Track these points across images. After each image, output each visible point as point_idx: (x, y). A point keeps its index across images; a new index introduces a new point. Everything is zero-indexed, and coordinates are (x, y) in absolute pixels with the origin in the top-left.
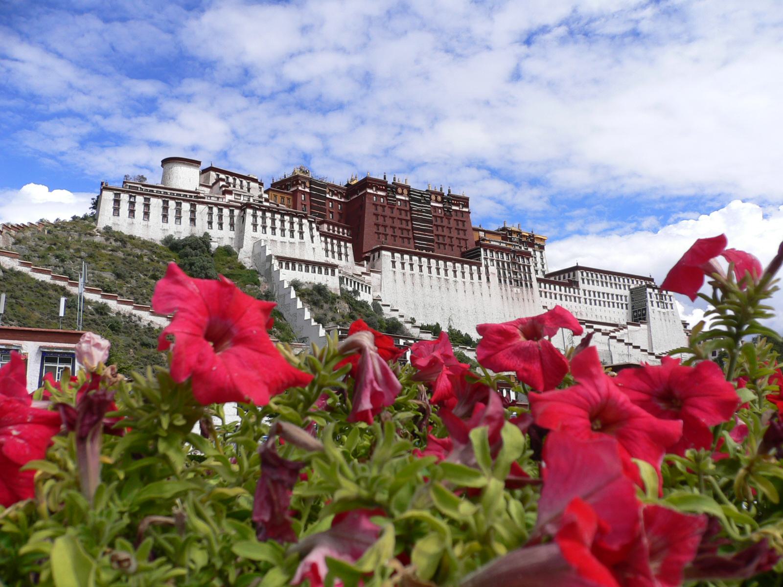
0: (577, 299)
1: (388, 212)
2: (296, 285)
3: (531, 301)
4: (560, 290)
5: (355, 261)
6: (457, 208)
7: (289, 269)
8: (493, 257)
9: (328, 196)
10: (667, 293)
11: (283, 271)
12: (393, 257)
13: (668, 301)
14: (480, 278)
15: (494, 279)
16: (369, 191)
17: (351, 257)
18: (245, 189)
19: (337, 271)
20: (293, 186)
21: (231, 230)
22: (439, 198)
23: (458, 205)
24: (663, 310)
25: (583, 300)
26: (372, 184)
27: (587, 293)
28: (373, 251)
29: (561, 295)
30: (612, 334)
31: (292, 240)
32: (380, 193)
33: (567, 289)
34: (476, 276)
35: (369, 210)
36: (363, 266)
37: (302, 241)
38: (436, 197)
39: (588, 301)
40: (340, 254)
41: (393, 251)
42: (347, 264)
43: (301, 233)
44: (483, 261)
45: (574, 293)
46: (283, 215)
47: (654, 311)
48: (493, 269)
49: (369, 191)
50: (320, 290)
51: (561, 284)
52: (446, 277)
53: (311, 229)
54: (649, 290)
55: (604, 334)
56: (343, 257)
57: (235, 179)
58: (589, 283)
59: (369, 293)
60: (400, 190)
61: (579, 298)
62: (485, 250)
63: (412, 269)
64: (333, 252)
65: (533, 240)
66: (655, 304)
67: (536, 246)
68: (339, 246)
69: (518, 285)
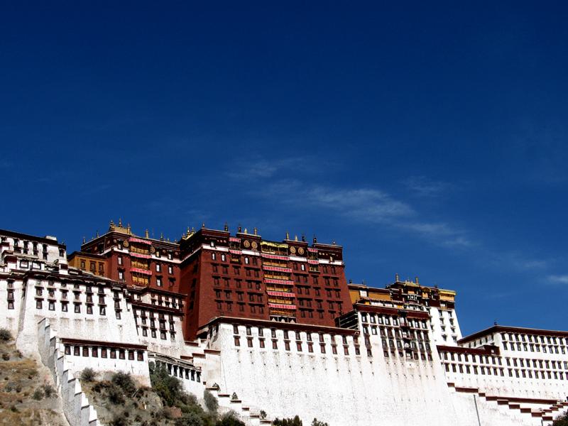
0: (498, 371)
2: (88, 376)
3: (431, 377)
4: (474, 361)
5: (185, 339)
6: (326, 262)
7: (124, 358)
8: (375, 322)
9: (154, 257)
11: (71, 358)
12: (236, 331)
15: (377, 350)
16: (206, 247)
17: (179, 335)
18: (40, 255)
19: (145, 355)
20: (108, 246)
21: (9, 308)
25: (506, 372)
26: (208, 237)
27: (512, 361)
28: (210, 325)
29: (475, 367)
30: (548, 414)
31: (89, 317)
32: (219, 249)
33: (484, 358)
34: (352, 349)
35: (206, 271)
36: (196, 345)
37: (104, 317)
38: (297, 249)
39: (514, 372)
40: (163, 331)
41: (236, 323)
42: (175, 346)
43: (102, 306)
44: (361, 328)
45: (494, 362)
46: (89, 286)
48: (376, 340)
49: (206, 247)
50: (122, 380)
51: (474, 352)
52: (311, 354)
53: (117, 300)
55: (534, 415)
57: (26, 244)
58: (513, 348)
59: (199, 381)
60: (247, 243)
61: (501, 369)
62: (364, 315)
64: (154, 330)
65: (437, 297)
67: (443, 305)
68: (162, 321)
69: (412, 358)
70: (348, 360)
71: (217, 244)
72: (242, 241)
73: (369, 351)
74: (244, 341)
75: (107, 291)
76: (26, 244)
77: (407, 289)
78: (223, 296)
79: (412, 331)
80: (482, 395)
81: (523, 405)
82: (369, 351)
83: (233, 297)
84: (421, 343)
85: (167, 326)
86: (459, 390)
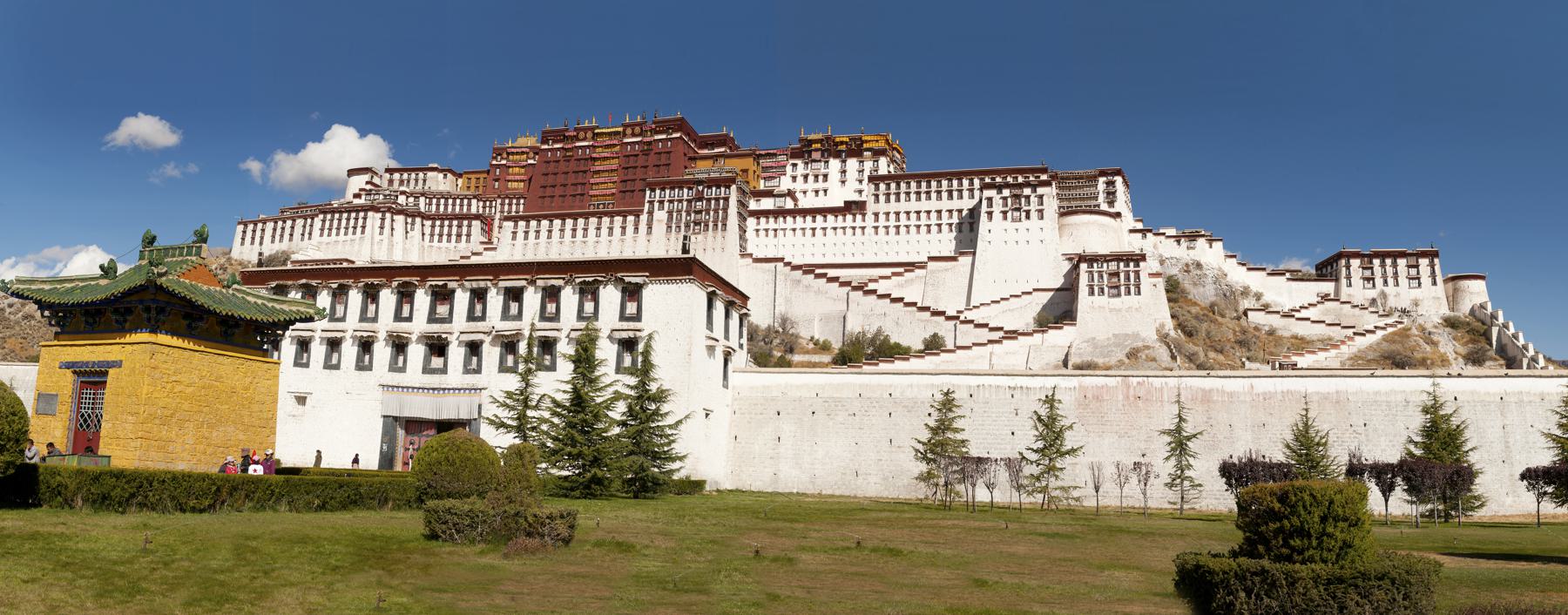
1: (563, 167)
3: (718, 250)
13: (1034, 206)
14: (636, 229)
22: (637, 130)
24: (1017, 225)
43: (364, 227)
47: (992, 230)
48: (661, 215)
54: (987, 193)
55: (843, 284)
56: (464, 238)
60: (582, 135)
62: (653, 190)
63: (537, 237)
66: (997, 216)
71: (555, 142)
74: (520, 235)
75: (370, 214)
77: (811, 142)
78: (549, 191)
79: (709, 200)
80: (788, 264)
83: (558, 191)
84: (716, 211)
85: (465, 230)
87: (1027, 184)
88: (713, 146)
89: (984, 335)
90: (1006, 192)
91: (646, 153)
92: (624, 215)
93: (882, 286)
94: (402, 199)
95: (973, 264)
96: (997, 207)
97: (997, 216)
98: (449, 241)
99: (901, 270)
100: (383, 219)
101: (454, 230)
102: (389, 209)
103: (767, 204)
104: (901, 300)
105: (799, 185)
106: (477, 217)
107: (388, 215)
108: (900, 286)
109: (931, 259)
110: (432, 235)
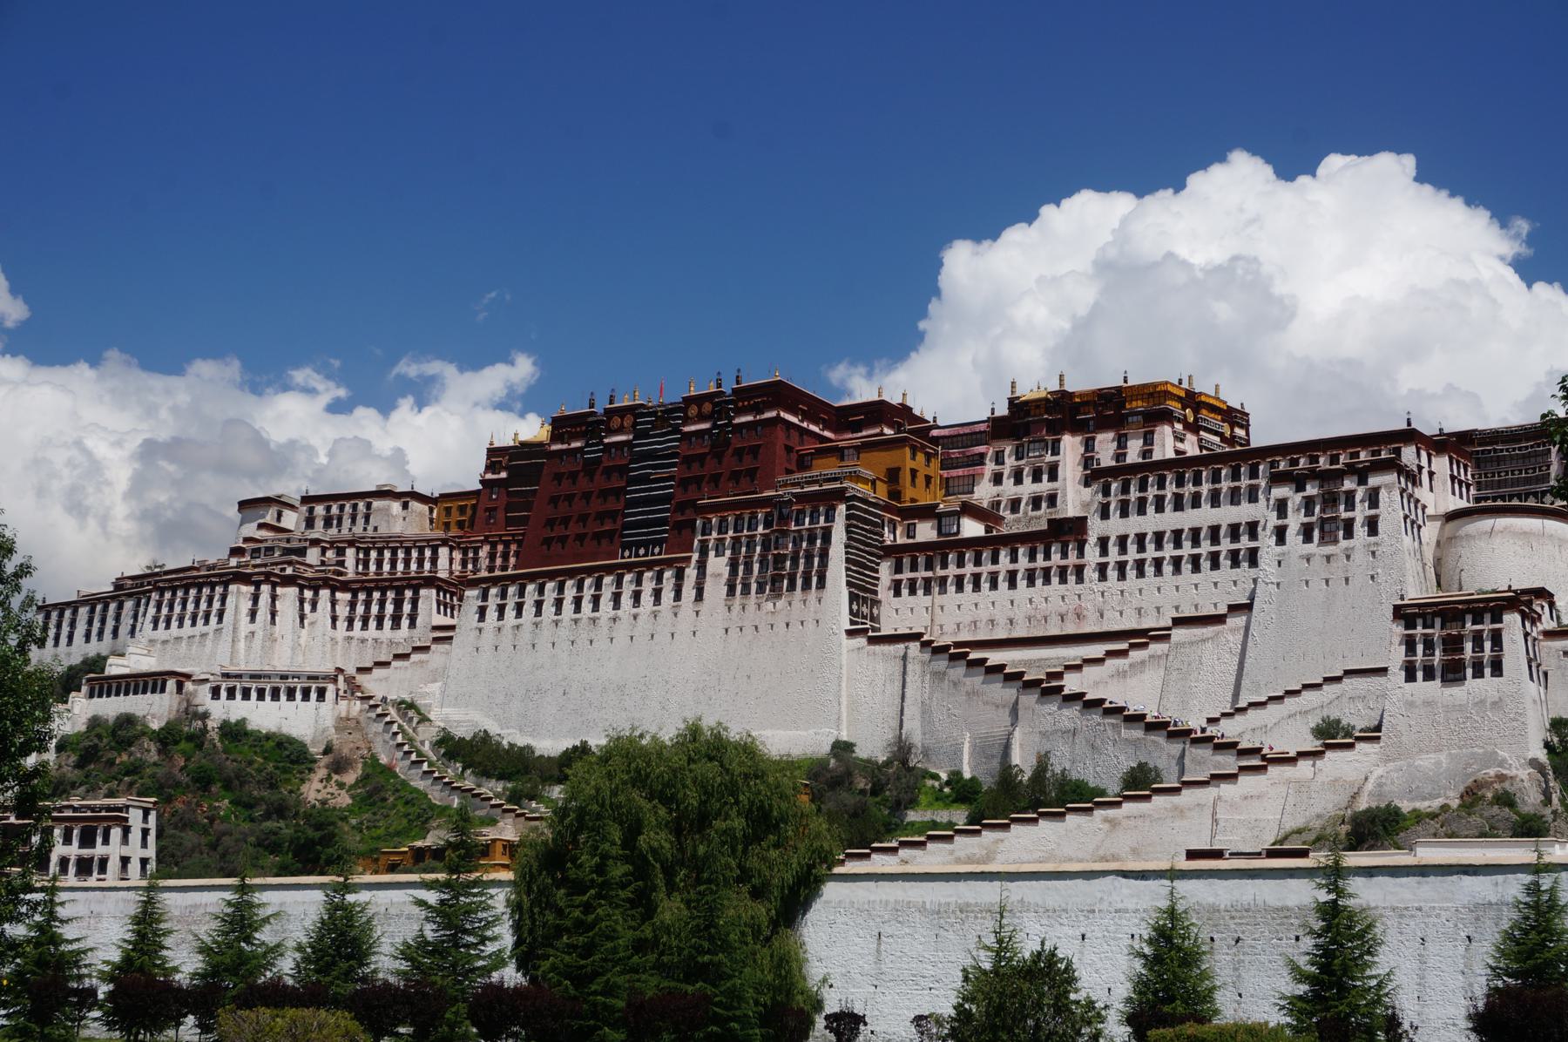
1: (583, 483)
3: (810, 625)
10: (1362, 481)
14: (678, 596)
15: (715, 589)
19: (171, 684)
22: (707, 407)
23: (758, 410)
24: (1329, 549)
34: (668, 595)
38: (700, 408)
48: (718, 565)
56: (405, 622)
57: (342, 508)
61: (1079, 570)
68: (398, 604)
70: (655, 615)
72: (610, 419)
73: (699, 596)
75: (233, 588)
76: (342, 508)
78: (559, 531)
81: (994, 657)
82: (699, 596)
83: (574, 529)
85: (407, 608)
86: (873, 641)
87: (1351, 470)
88: (857, 427)
89: (1229, 763)
90: (1311, 490)
91: (718, 455)
92: (659, 567)
93: (1071, 683)
94: (313, 556)
95: (1247, 628)
96: (1295, 521)
97: (1293, 535)
98: (380, 626)
99: (1124, 646)
100: (255, 598)
101: (389, 608)
102: (267, 577)
103: (926, 532)
104: (1098, 703)
105: (1008, 488)
106: (431, 582)
107: (265, 588)
108: (1121, 674)
109: (1179, 622)
110: (350, 621)
